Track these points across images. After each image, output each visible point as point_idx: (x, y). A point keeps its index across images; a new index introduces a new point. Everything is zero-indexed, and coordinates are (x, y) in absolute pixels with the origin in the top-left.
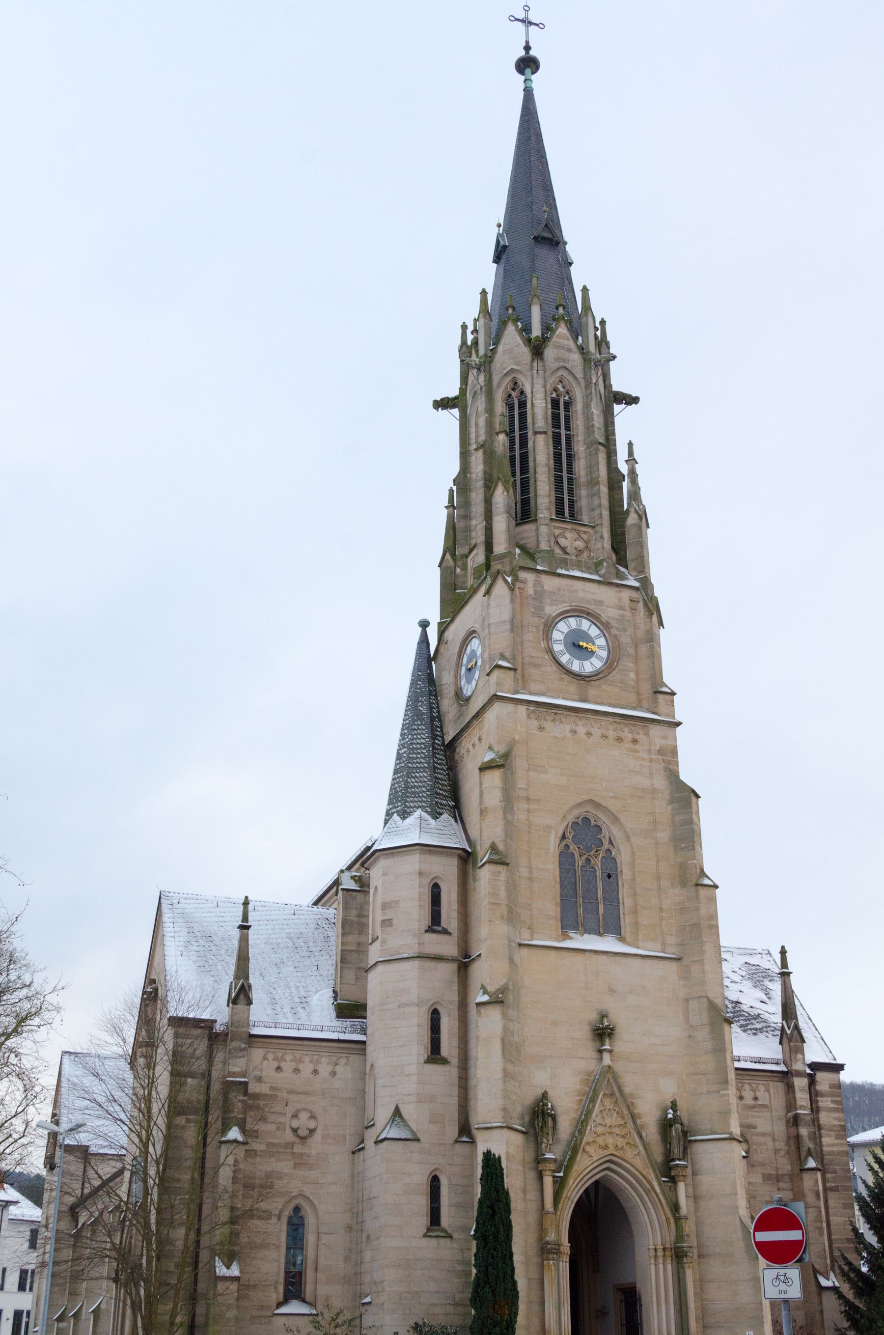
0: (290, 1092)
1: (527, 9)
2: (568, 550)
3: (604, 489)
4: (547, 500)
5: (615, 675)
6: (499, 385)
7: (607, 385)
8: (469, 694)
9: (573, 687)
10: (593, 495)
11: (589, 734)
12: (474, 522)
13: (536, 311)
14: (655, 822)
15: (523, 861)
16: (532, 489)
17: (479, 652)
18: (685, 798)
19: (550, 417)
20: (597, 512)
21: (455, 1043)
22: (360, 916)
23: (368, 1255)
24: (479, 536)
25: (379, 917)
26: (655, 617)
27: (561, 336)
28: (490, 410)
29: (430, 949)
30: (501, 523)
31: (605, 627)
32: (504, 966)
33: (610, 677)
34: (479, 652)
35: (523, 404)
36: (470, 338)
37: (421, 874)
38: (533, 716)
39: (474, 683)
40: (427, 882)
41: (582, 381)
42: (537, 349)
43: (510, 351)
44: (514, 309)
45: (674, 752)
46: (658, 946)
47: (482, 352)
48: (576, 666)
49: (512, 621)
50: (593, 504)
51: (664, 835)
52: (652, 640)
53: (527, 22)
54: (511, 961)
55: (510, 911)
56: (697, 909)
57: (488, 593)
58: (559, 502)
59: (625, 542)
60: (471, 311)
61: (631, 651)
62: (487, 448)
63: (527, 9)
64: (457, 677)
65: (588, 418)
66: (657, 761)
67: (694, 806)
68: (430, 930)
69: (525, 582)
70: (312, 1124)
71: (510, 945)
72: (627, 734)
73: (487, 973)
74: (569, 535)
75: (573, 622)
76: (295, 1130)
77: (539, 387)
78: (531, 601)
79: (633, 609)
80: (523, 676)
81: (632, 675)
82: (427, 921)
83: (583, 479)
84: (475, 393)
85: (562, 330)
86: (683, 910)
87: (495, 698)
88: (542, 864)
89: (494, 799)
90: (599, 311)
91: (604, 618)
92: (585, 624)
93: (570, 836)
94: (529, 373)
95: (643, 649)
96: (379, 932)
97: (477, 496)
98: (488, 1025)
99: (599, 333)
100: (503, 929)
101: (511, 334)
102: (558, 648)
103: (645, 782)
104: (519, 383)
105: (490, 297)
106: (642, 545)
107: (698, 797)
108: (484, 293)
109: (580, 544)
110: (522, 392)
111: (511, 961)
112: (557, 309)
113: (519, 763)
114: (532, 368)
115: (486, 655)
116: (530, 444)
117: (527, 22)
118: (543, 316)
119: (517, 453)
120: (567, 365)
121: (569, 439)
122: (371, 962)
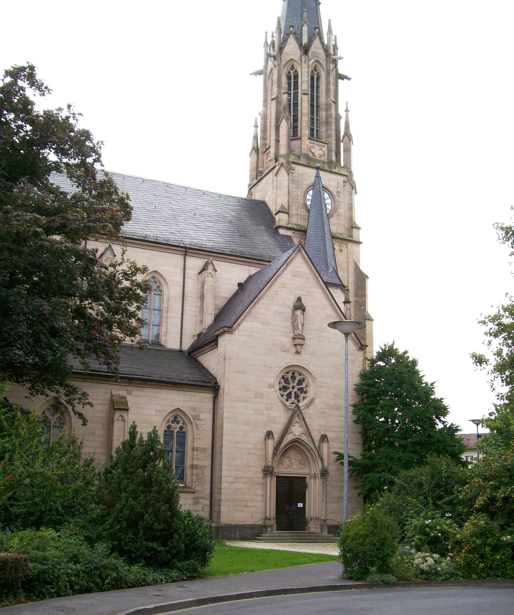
6: (284, 66)
7: (337, 70)
13: (305, 29)
35: (296, 77)
44: (293, 27)
60: (273, 27)
74: (316, 147)
77: (305, 70)
101: (292, 40)
104: (295, 66)
107: (368, 278)
110: (296, 71)
116: (299, 99)
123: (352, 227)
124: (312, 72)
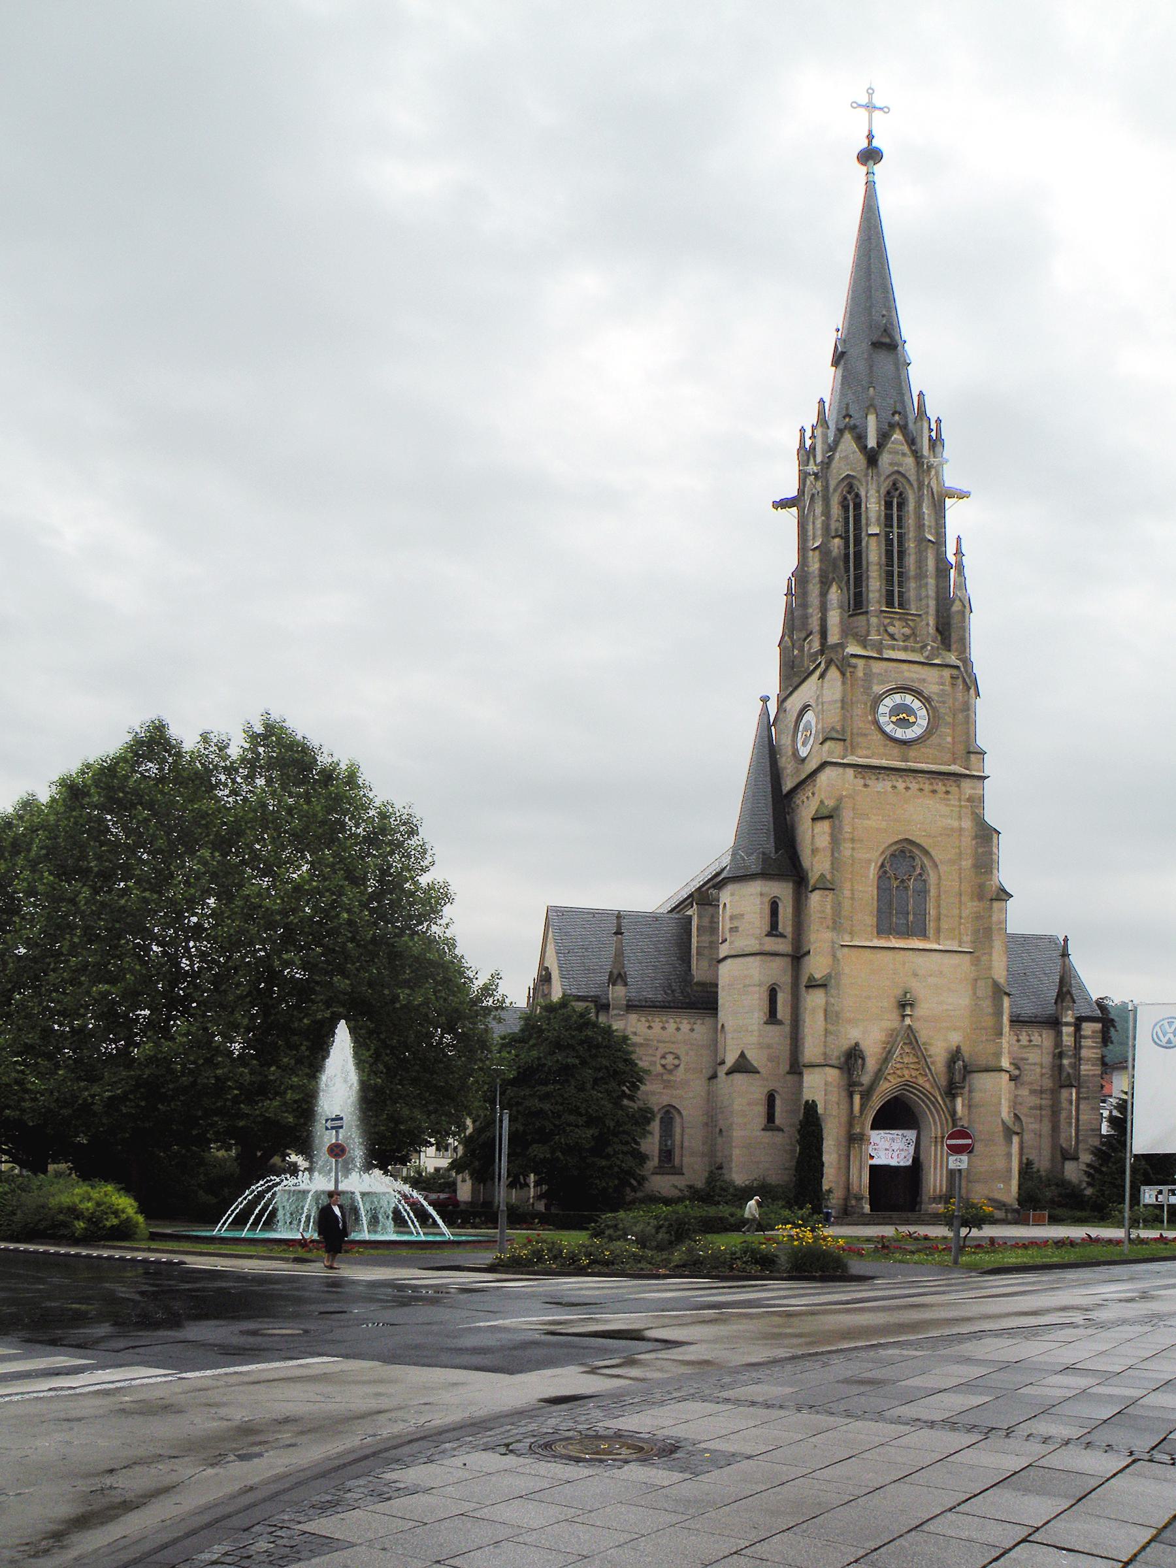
0: (658, 1041)
1: (870, 92)
2: (896, 637)
3: (932, 581)
4: (877, 594)
5: (934, 739)
6: (835, 490)
8: (805, 755)
9: (896, 751)
10: (920, 587)
11: (907, 788)
12: (810, 610)
13: (872, 420)
14: (960, 853)
15: (848, 885)
16: (864, 584)
17: (813, 724)
18: (986, 835)
19: (883, 518)
20: (924, 602)
21: (788, 1010)
22: (711, 922)
23: (719, 1140)
24: (814, 624)
25: (728, 926)
26: (972, 691)
27: (896, 442)
28: (827, 513)
29: (767, 948)
30: (834, 618)
31: (926, 700)
32: (830, 960)
33: (928, 742)
34: (813, 724)
35: (857, 506)
36: (808, 443)
37: (761, 895)
38: (859, 776)
39: (809, 747)
40: (766, 899)
41: (915, 484)
42: (872, 459)
43: (846, 457)
45: (981, 799)
46: (956, 943)
47: (819, 459)
48: (899, 733)
49: (842, 701)
50: (922, 598)
51: (967, 863)
52: (967, 709)
53: (870, 107)
54: (834, 956)
55: (834, 922)
56: (990, 916)
57: (822, 676)
58: (890, 594)
59: (950, 627)
60: (810, 418)
61: (949, 719)
62: (823, 550)
63: (870, 92)
64: (794, 741)
65: (919, 516)
66: (966, 807)
67: (995, 841)
68: (769, 935)
69: (855, 667)
70: (676, 1062)
71: (833, 947)
72: (940, 787)
73: (817, 966)
74: (897, 623)
75: (897, 698)
76: (663, 1066)
77: (872, 492)
78: (860, 683)
79: (953, 685)
80: (851, 744)
81: (949, 739)
82: (766, 927)
83: (912, 573)
84: (813, 495)
85: (897, 436)
86: (978, 917)
87: (824, 765)
88: (862, 888)
89: (823, 841)
90: (932, 412)
91: (926, 693)
92: (909, 699)
93: (888, 865)
94: (863, 480)
95: (960, 717)
96: (728, 936)
97: (814, 589)
98: (814, 1000)
99: (933, 434)
100: (829, 935)
102: (882, 720)
103: (955, 824)
105: (827, 406)
106: (964, 629)
108: (822, 401)
109: (907, 631)
111: (834, 956)
112: (893, 415)
113: (847, 815)
114: (866, 475)
115: (819, 726)
116: (864, 544)
117: (870, 107)
118: (879, 430)
119: (852, 550)
120: (901, 469)
121: (900, 536)
122: (721, 956)
123: (969, 752)
124: (888, 493)
